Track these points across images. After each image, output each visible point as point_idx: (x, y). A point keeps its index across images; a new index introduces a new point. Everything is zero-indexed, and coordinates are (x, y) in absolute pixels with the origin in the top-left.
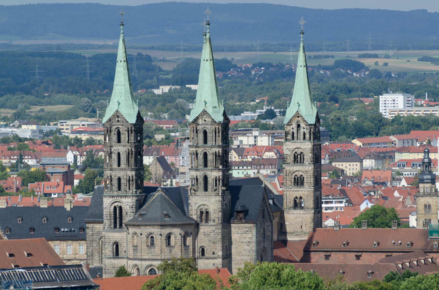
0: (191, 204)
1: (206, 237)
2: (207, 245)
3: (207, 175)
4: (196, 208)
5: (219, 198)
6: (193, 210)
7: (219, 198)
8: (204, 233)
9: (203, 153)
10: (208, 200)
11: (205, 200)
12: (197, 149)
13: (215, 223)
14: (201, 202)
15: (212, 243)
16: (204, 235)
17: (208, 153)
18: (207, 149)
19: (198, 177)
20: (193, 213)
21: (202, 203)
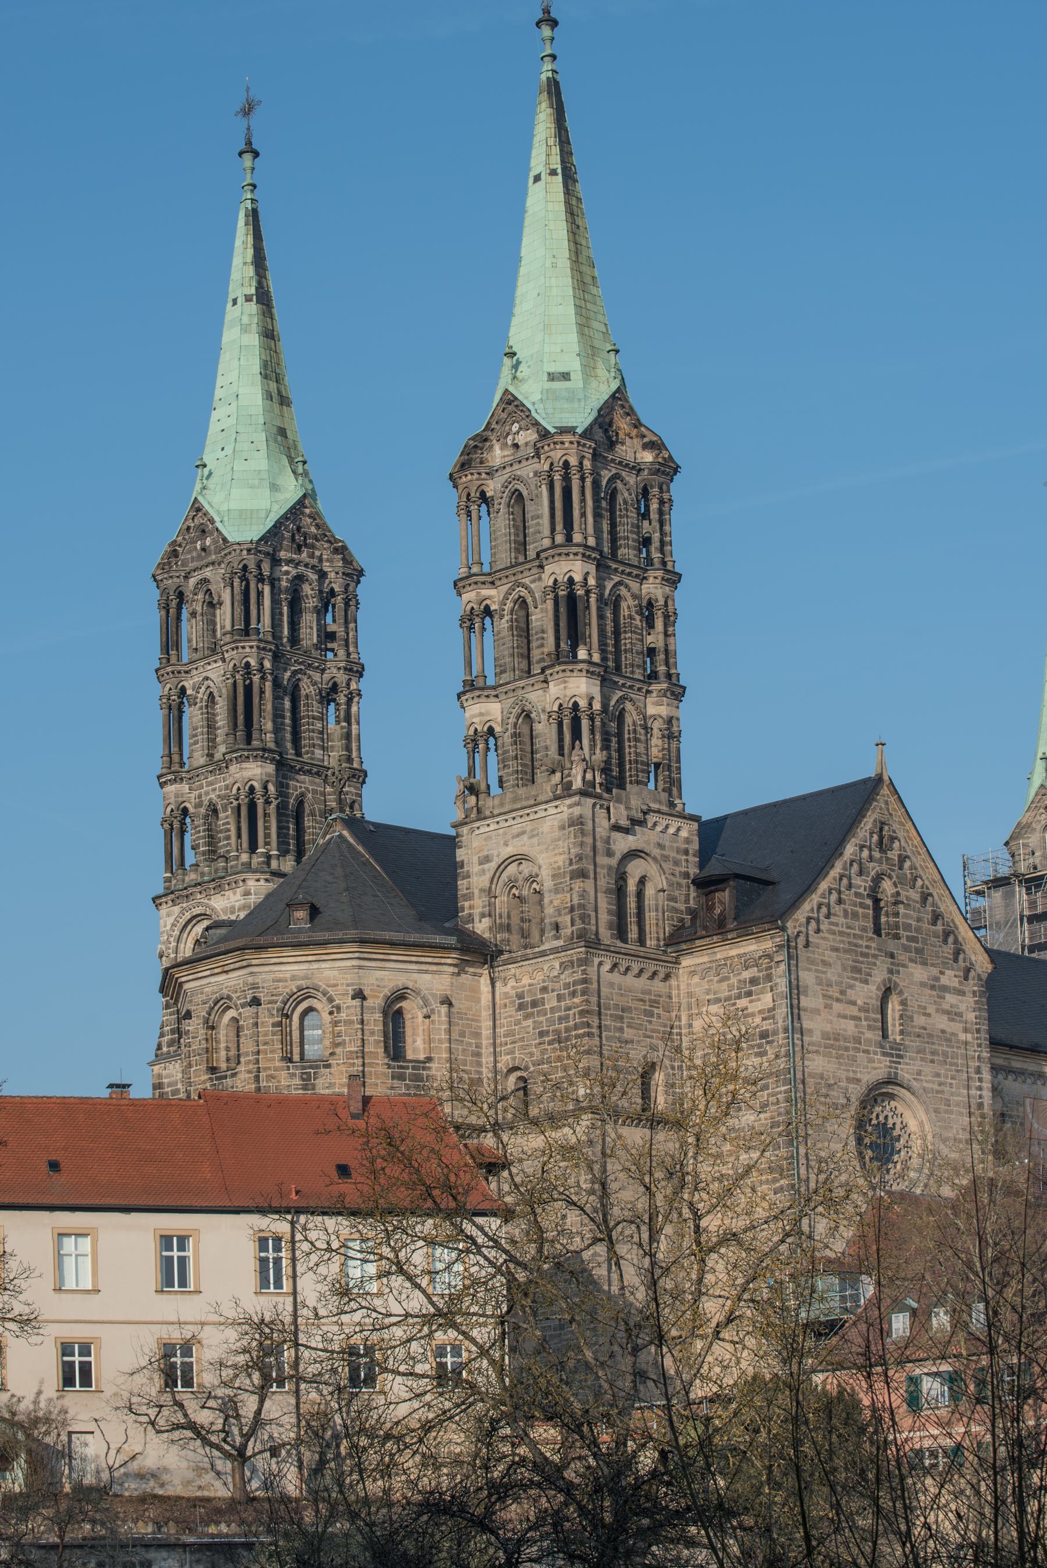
0: (466, 869)
1: (527, 1017)
2: (532, 1054)
3: (528, 707)
4: (484, 881)
5: (570, 806)
6: (476, 892)
7: (570, 806)
8: (520, 996)
9: (509, 605)
10: (528, 828)
11: (518, 835)
12: (486, 592)
13: (557, 938)
14: (506, 844)
15: (550, 1043)
16: (521, 1007)
17: (529, 600)
18: (527, 581)
19: (498, 729)
20: (476, 912)
21: (510, 850)
